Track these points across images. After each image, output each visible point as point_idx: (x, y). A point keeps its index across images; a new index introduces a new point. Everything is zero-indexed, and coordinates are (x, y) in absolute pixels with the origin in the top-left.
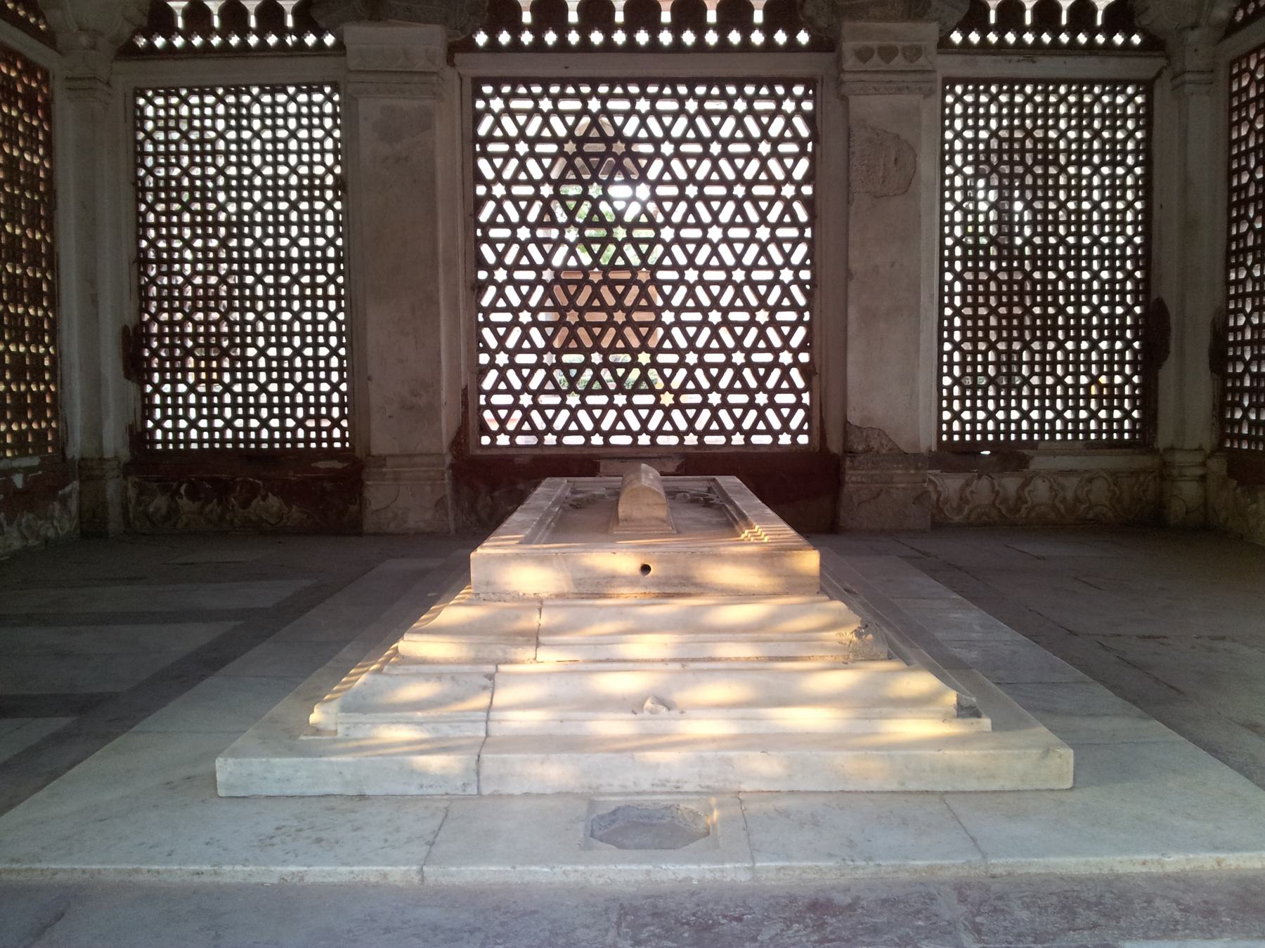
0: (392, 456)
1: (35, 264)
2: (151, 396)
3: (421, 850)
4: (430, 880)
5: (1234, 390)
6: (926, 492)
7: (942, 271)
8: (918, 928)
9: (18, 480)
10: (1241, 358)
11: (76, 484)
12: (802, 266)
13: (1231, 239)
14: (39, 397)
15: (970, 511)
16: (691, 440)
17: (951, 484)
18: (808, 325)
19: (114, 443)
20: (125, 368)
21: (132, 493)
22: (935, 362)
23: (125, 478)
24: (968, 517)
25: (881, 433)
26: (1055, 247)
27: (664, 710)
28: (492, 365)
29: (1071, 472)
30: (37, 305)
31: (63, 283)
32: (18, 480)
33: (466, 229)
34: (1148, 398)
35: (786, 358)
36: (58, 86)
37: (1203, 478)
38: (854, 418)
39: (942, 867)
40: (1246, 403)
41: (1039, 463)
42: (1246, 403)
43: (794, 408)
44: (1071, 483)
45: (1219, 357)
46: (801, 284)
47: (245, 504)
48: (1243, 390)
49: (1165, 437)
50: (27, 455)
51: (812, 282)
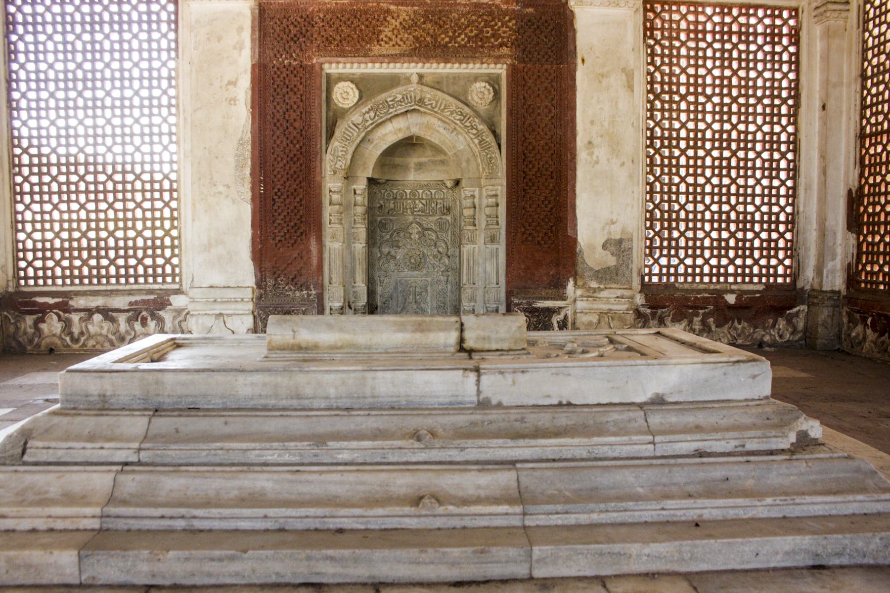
11: (803, 308)
32: (731, 299)
36: (804, 18)
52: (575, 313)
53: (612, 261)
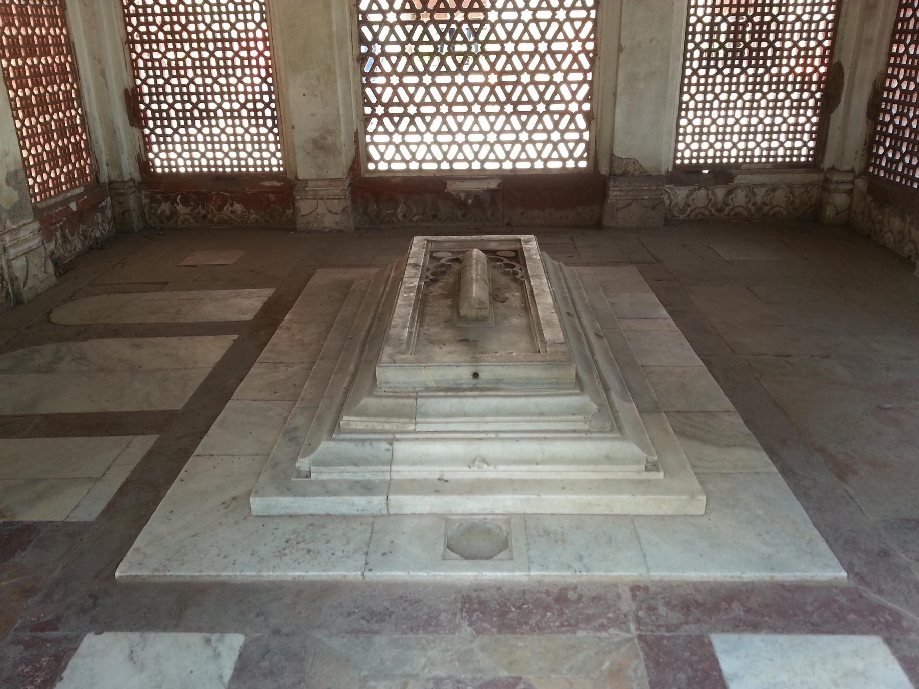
0: (312, 180)
1: (60, 53)
2: (148, 136)
3: (360, 559)
4: (367, 579)
5: (881, 133)
6: (662, 201)
7: (687, 42)
8: (610, 618)
9: (73, 206)
10: (890, 112)
12: (588, 39)
13: (898, 20)
14: (77, 144)
15: (692, 211)
16: (508, 166)
17: (681, 193)
18: (591, 83)
19: (129, 169)
20: (130, 119)
21: (145, 201)
22: (673, 140)
23: (139, 192)
24: (689, 216)
25: (635, 162)
26: (769, 24)
27: (486, 466)
28: (373, 114)
29: (763, 185)
30: (66, 81)
31: (79, 60)
32: (73, 206)
33: (351, 16)
34: (821, 134)
35: (574, 107)
37: (850, 192)
38: (618, 153)
39: (626, 576)
40: (887, 145)
41: (740, 179)
42: (887, 145)
43: (577, 142)
44: (760, 193)
45: (874, 109)
46: (587, 53)
47: (220, 208)
48: (886, 135)
49: (827, 163)
50: (76, 187)
51: (595, 51)
52: (8, 261)
53: (15, 196)
